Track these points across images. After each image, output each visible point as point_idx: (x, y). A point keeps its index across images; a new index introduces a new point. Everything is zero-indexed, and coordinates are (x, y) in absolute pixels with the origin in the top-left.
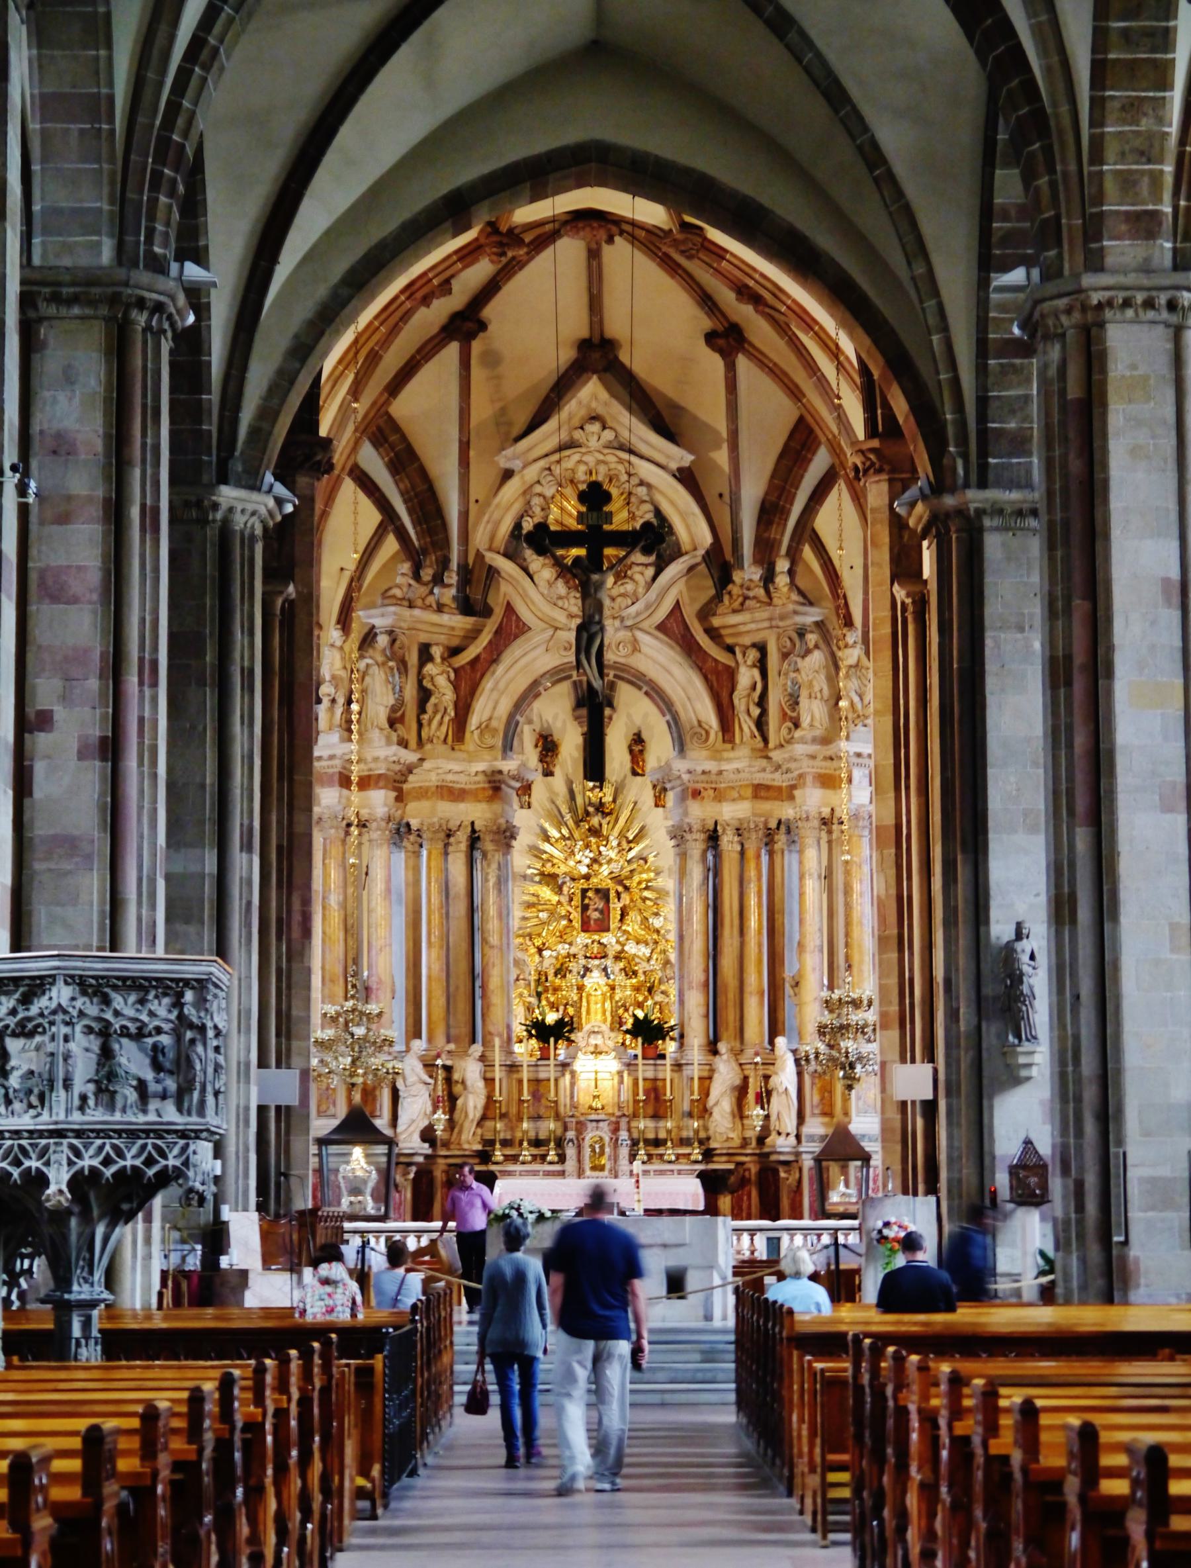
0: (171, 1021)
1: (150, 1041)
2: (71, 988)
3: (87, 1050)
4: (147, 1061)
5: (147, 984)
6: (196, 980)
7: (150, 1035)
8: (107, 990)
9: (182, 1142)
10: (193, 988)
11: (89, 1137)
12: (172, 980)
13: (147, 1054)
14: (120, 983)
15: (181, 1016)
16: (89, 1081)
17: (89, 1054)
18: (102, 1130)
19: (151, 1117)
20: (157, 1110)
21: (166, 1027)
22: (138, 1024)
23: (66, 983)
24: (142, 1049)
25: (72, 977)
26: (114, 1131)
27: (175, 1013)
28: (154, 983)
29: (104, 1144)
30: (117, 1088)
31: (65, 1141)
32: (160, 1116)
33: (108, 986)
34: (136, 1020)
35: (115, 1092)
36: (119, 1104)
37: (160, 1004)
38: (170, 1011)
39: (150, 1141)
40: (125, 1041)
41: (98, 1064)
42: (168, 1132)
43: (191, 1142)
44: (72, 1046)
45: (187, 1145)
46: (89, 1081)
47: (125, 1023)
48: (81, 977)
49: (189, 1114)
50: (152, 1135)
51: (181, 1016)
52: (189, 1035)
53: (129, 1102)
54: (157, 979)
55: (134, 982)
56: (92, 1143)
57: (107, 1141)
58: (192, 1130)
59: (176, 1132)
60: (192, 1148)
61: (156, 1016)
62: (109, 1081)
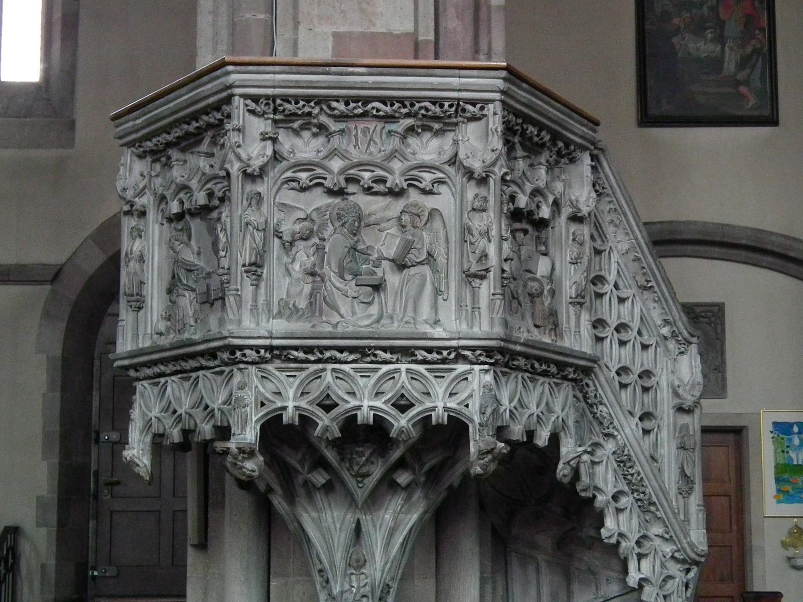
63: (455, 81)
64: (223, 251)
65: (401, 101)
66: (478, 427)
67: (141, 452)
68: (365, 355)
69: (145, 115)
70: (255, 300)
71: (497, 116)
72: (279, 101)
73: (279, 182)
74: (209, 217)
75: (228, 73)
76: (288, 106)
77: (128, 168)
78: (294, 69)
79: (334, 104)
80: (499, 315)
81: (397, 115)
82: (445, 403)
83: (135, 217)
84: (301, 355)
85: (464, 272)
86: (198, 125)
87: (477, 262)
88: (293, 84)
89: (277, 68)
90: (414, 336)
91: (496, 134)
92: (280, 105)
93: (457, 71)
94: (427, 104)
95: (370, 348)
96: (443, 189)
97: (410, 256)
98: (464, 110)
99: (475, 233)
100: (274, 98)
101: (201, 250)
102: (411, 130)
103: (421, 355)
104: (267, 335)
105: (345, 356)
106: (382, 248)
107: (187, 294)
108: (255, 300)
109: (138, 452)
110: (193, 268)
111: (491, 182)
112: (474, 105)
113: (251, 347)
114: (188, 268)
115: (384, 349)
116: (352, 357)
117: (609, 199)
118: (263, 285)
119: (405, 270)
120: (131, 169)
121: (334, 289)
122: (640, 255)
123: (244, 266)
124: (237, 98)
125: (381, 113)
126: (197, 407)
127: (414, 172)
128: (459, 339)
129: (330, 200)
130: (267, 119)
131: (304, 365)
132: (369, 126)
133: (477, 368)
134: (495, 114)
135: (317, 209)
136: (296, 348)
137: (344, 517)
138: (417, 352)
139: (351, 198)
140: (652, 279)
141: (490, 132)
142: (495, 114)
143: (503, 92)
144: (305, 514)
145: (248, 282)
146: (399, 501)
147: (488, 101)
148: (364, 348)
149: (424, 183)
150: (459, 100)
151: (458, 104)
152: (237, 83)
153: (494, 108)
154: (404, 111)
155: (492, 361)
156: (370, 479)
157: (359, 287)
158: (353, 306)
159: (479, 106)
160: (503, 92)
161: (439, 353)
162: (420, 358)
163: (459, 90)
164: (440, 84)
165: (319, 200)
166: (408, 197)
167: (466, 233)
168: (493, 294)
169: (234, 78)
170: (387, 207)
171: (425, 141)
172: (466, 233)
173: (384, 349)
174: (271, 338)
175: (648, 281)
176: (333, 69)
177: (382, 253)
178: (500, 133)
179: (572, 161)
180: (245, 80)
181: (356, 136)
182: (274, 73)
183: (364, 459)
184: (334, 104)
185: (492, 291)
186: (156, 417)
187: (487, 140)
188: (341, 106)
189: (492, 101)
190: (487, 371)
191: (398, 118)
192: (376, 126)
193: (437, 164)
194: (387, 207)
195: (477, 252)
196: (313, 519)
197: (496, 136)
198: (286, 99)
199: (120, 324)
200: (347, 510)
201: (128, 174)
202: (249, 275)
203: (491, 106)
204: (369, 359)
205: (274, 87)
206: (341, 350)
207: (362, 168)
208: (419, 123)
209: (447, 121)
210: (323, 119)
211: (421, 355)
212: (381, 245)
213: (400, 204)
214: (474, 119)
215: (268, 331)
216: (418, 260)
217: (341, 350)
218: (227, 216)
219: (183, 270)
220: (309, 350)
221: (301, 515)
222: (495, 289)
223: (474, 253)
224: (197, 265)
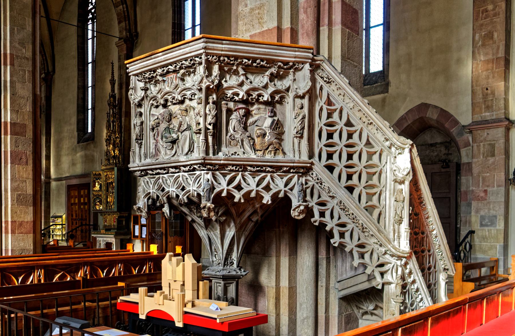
63: (187, 50)
70: (140, 153)
72: (143, 74)
73: (150, 106)
78: (143, 60)
80: (202, 149)
81: (177, 69)
88: (143, 67)
93: (187, 45)
94: (184, 62)
97: (181, 128)
102: (184, 75)
108: (140, 153)
112: (198, 57)
115: (172, 167)
116: (164, 172)
117: (335, 83)
118: (143, 146)
122: (360, 108)
124: (132, 76)
127: (183, 92)
128: (190, 161)
129: (164, 110)
133: (203, 172)
139: (169, 107)
140: (370, 119)
143: (205, 48)
145: (137, 144)
147: (201, 54)
148: (165, 167)
150: (192, 56)
155: (206, 169)
158: (166, 151)
163: (190, 52)
165: (161, 110)
173: (172, 167)
174: (139, 167)
175: (369, 120)
176: (153, 56)
179: (297, 70)
190: (207, 173)
191: (179, 70)
193: (190, 87)
198: (145, 72)
206: (161, 169)
207: (168, 94)
208: (186, 71)
213: (183, 107)
216: (183, 129)
217: (161, 169)
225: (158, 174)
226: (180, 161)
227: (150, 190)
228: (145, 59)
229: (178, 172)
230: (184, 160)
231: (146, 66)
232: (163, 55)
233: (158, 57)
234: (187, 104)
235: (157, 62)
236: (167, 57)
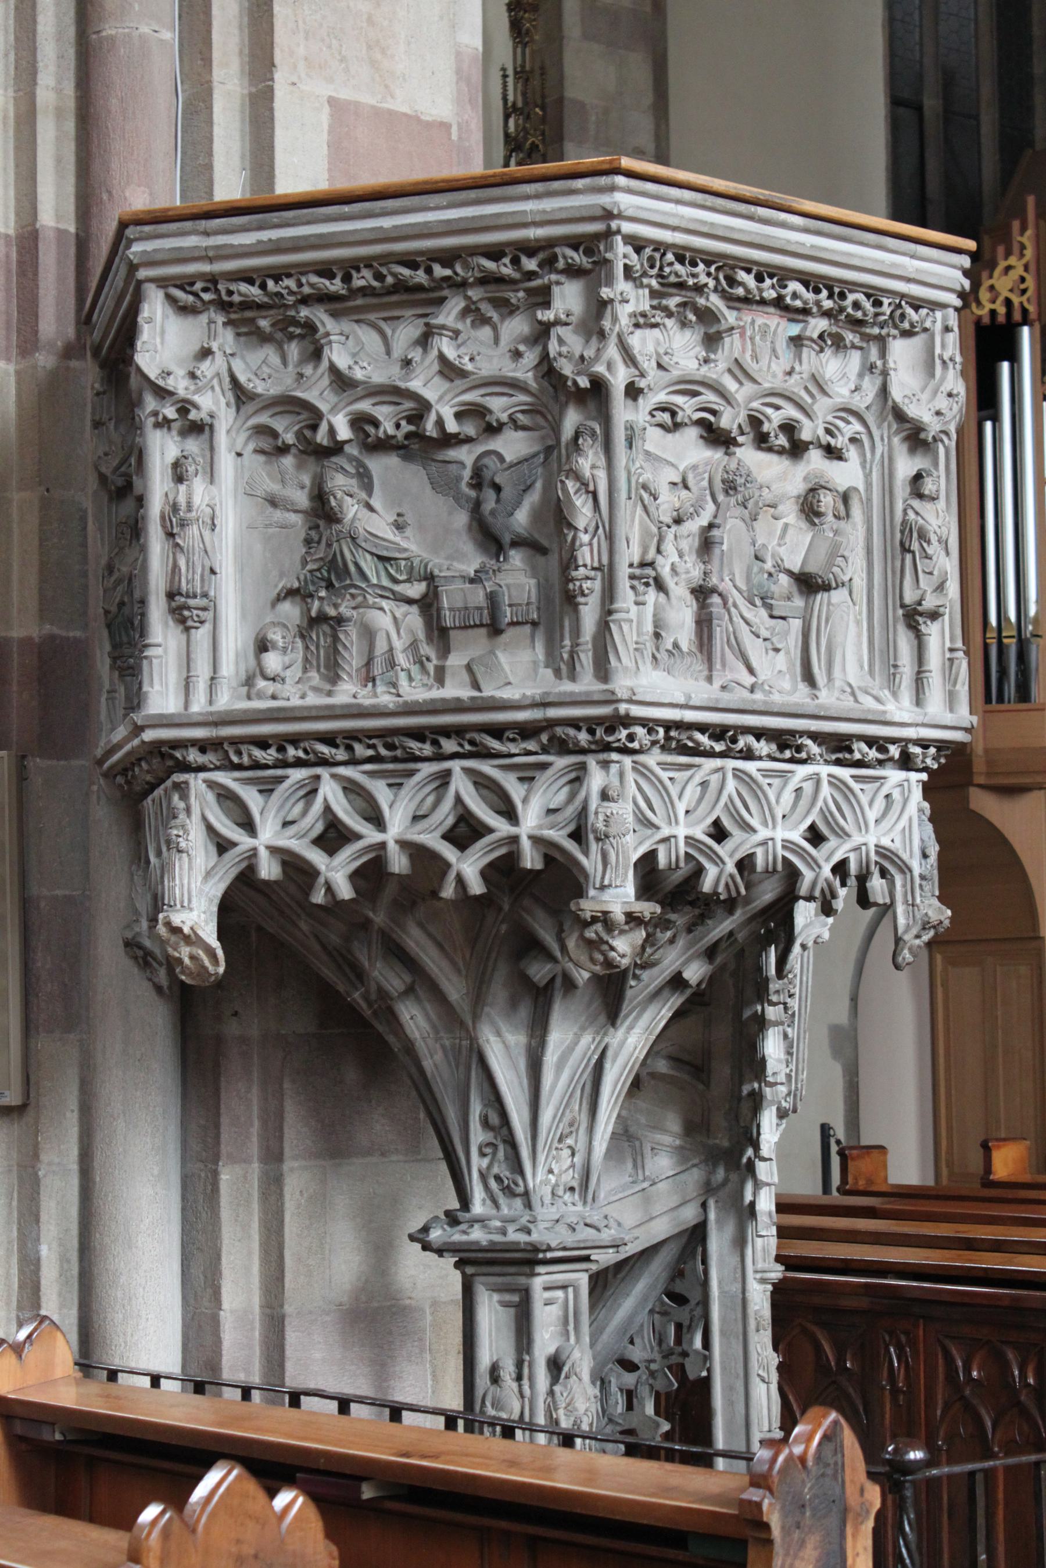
0: (515, 385)
1: (466, 455)
2: (204, 318)
3: (273, 502)
4: (462, 519)
5: (420, 277)
6: (575, 243)
7: (449, 440)
8: (304, 312)
9: (561, 762)
10: (573, 272)
11: (256, 766)
12: (495, 253)
13: (458, 498)
14: (336, 286)
15: (547, 369)
16: (278, 599)
17: (278, 515)
18: (295, 740)
19: (456, 690)
20: (469, 668)
21: (499, 406)
22: (409, 405)
23: (184, 310)
24: (444, 485)
25: (185, 283)
26: (329, 739)
27: (531, 357)
28: (439, 271)
29: (318, 778)
30: (345, 610)
31: (197, 783)
32: (476, 686)
33: (305, 301)
34: (393, 393)
35: (340, 620)
36: (353, 658)
37: (497, 340)
38: (517, 355)
39: (456, 765)
40: (380, 465)
41: (308, 542)
42: (497, 731)
43: (591, 762)
44: (199, 491)
45: (583, 767)
46: (278, 599)
47: (364, 406)
48: (212, 281)
49: (573, 677)
50: (449, 746)
51: (547, 369)
52: (572, 419)
53: (381, 646)
54: (448, 257)
55: (379, 277)
56: (280, 780)
57: (323, 772)
58: (574, 723)
59: (526, 731)
60: (596, 780)
61: (463, 374)
62: (330, 586)
64: (586, 531)
65: (829, 284)
66: (917, 881)
67: (203, 916)
68: (782, 748)
69: (260, 228)
71: (951, 334)
74: (440, 457)
75: (613, 188)
76: (678, 267)
77: (158, 329)
78: (710, 200)
79: (742, 275)
82: (878, 838)
83: (174, 433)
84: (704, 739)
85: (903, 606)
86: (448, 272)
87: (935, 591)
88: (705, 229)
89: (687, 195)
90: (870, 717)
91: (951, 365)
92: (671, 264)
95: (793, 733)
96: (852, 453)
98: (903, 316)
99: (934, 538)
100: (661, 247)
101: (409, 518)
103: (860, 750)
104: (682, 700)
105: (763, 747)
106: (782, 551)
107: (384, 603)
109: (199, 916)
110: (397, 555)
111: (941, 450)
113: (643, 722)
114: (385, 553)
119: (819, 597)
120: (163, 332)
121: (741, 621)
123: (631, 565)
125: (798, 303)
126: (430, 832)
130: (642, 286)
131: (697, 760)
132: (768, 322)
134: (947, 329)
135: (695, 467)
136: (702, 728)
137: (576, 1043)
138: (855, 746)
141: (938, 362)
142: (947, 329)
144: (492, 1038)
146: (663, 1011)
149: (840, 438)
150: (903, 296)
151: (899, 306)
152: (630, 213)
153: (945, 319)
154: (828, 304)
156: (655, 970)
157: (774, 621)
159: (923, 312)
160: (962, 295)
161: (883, 749)
162: (857, 756)
163: (909, 280)
164: (894, 265)
166: (808, 462)
167: (915, 535)
168: (951, 650)
169: (624, 201)
170: (783, 477)
171: (824, 361)
172: (915, 535)
176: (762, 211)
177: (782, 560)
178: (958, 367)
180: (641, 208)
181: (752, 339)
182: (678, 202)
183: (669, 934)
184: (742, 275)
185: (948, 645)
186: (268, 847)
187: (932, 375)
188: (749, 280)
189: (943, 306)
192: (778, 324)
194: (783, 477)
195: (935, 573)
196: (507, 1047)
197: (951, 373)
199: (150, 652)
200: (583, 1028)
201: (158, 340)
202: (636, 583)
203: (939, 314)
204: (788, 754)
205: (675, 229)
209: (868, 330)
210: (715, 301)
211: (860, 750)
212: (780, 545)
214: (907, 334)
215: (685, 694)
218: (593, 467)
219: (368, 557)
220: (719, 733)
221: (488, 1041)
222: (952, 639)
223: (931, 573)
224: (406, 550)
225: (697, 751)
226: (889, 718)
227: (688, 825)
228: (720, 202)
229: (722, 755)
230: (906, 717)
231: (720, 233)
232: (806, 230)
233: (783, 225)
234: (812, 466)
235: (778, 245)
236: (825, 249)
